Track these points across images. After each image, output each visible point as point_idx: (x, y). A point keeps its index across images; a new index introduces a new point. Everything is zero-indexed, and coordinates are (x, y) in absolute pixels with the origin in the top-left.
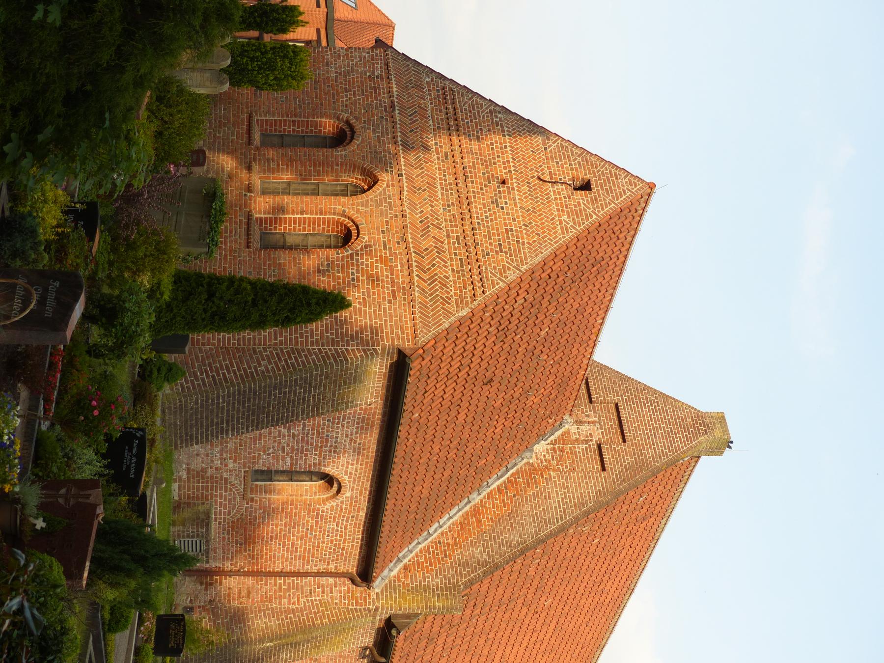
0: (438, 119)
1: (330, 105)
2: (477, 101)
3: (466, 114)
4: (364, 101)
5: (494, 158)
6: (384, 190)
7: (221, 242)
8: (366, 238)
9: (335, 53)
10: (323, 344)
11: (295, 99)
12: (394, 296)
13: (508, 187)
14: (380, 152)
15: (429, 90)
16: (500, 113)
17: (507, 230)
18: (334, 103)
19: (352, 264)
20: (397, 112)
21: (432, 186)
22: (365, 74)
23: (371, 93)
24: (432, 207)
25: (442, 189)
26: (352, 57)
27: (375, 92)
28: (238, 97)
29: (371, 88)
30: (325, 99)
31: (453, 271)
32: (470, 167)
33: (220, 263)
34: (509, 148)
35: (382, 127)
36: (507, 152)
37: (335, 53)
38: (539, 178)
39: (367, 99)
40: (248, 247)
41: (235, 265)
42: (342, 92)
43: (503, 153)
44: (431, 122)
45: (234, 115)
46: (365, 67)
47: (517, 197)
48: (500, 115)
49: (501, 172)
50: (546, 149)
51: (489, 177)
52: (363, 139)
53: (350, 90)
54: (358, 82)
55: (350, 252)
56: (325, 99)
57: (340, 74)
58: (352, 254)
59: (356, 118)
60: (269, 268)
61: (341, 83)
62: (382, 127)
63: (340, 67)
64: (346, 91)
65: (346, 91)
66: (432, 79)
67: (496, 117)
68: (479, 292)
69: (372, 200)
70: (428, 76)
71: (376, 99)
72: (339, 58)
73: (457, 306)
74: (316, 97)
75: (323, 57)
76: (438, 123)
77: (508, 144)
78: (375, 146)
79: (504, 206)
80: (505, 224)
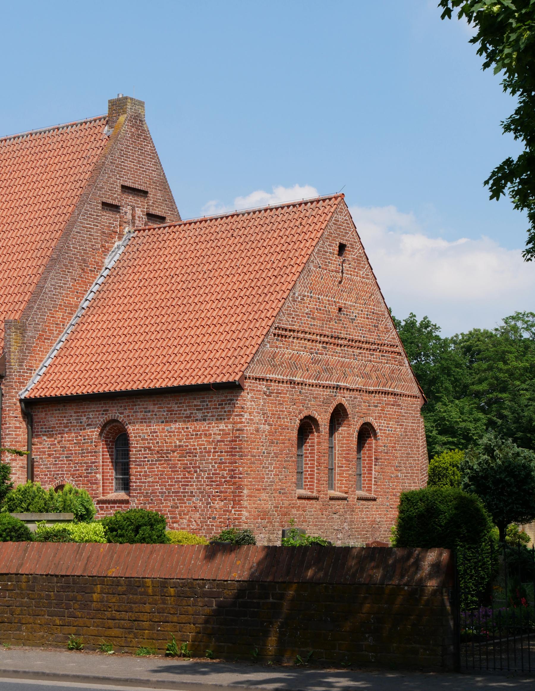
0: (299, 347)
1: (289, 433)
2: (285, 310)
3: (295, 322)
4: (288, 405)
5: (326, 311)
6: (347, 400)
7: (372, 517)
8: (371, 418)
9: (248, 423)
10: (419, 454)
11: (285, 461)
12: (399, 405)
13: (345, 308)
14: (324, 399)
15: (277, 347)
16: (294, 294)
17: (368, 318)
18: (288, 429)
19: (385, 430)
20: (294, 378)
21: (343, 365)
22: (265, 399)
23: (281, 397)
24: (354, 367)
25: (345, 357)
26: (251, 408)
27: (280, 393)
28: (285, 507)
29: (278, 397)
30: (285, 436)
31: (387, 363)
32: (332, 332)
33: (383, 518)
34: (320, 296)
35: (307, 393)
36: (322, 300)
37: (248, 423)
38: (340, 282)
39: (286, 401)
40: (358, 499)
41: (383, 508)
42: (280, 421)
43: (323, 303)
44: (302, 353)
45: (297, 511)
46: (259, 398)
47: (349, 303)
48: (297, 295)
49: (334, 310)
50: (320, 267)
51: (338, 320)
52: (315, 410)
53: (279, 415)
54: (272, 407)
55: (378, 430)
56: (285, 436)
57: (266, 421)
58: (380, 430)
59: (300, 413)
60: (385, 485)
61: (273, 421)
62: (307, 393)
63: (260, 420)
64: (280, 418)
65: (280, 418)
66: (269, 342)
67: (297, 298)
68: (397, 350)
69: (352, 411)
70: (266, 345)
71: (286, 394)
72: (252, 420)
73: (402, 366)
74: (284, 443)
75: (252, 434)
76: (302, 347)
77: (317, 296)
78: (320, 401)
79: (354, 315)
80: (364, 318)
